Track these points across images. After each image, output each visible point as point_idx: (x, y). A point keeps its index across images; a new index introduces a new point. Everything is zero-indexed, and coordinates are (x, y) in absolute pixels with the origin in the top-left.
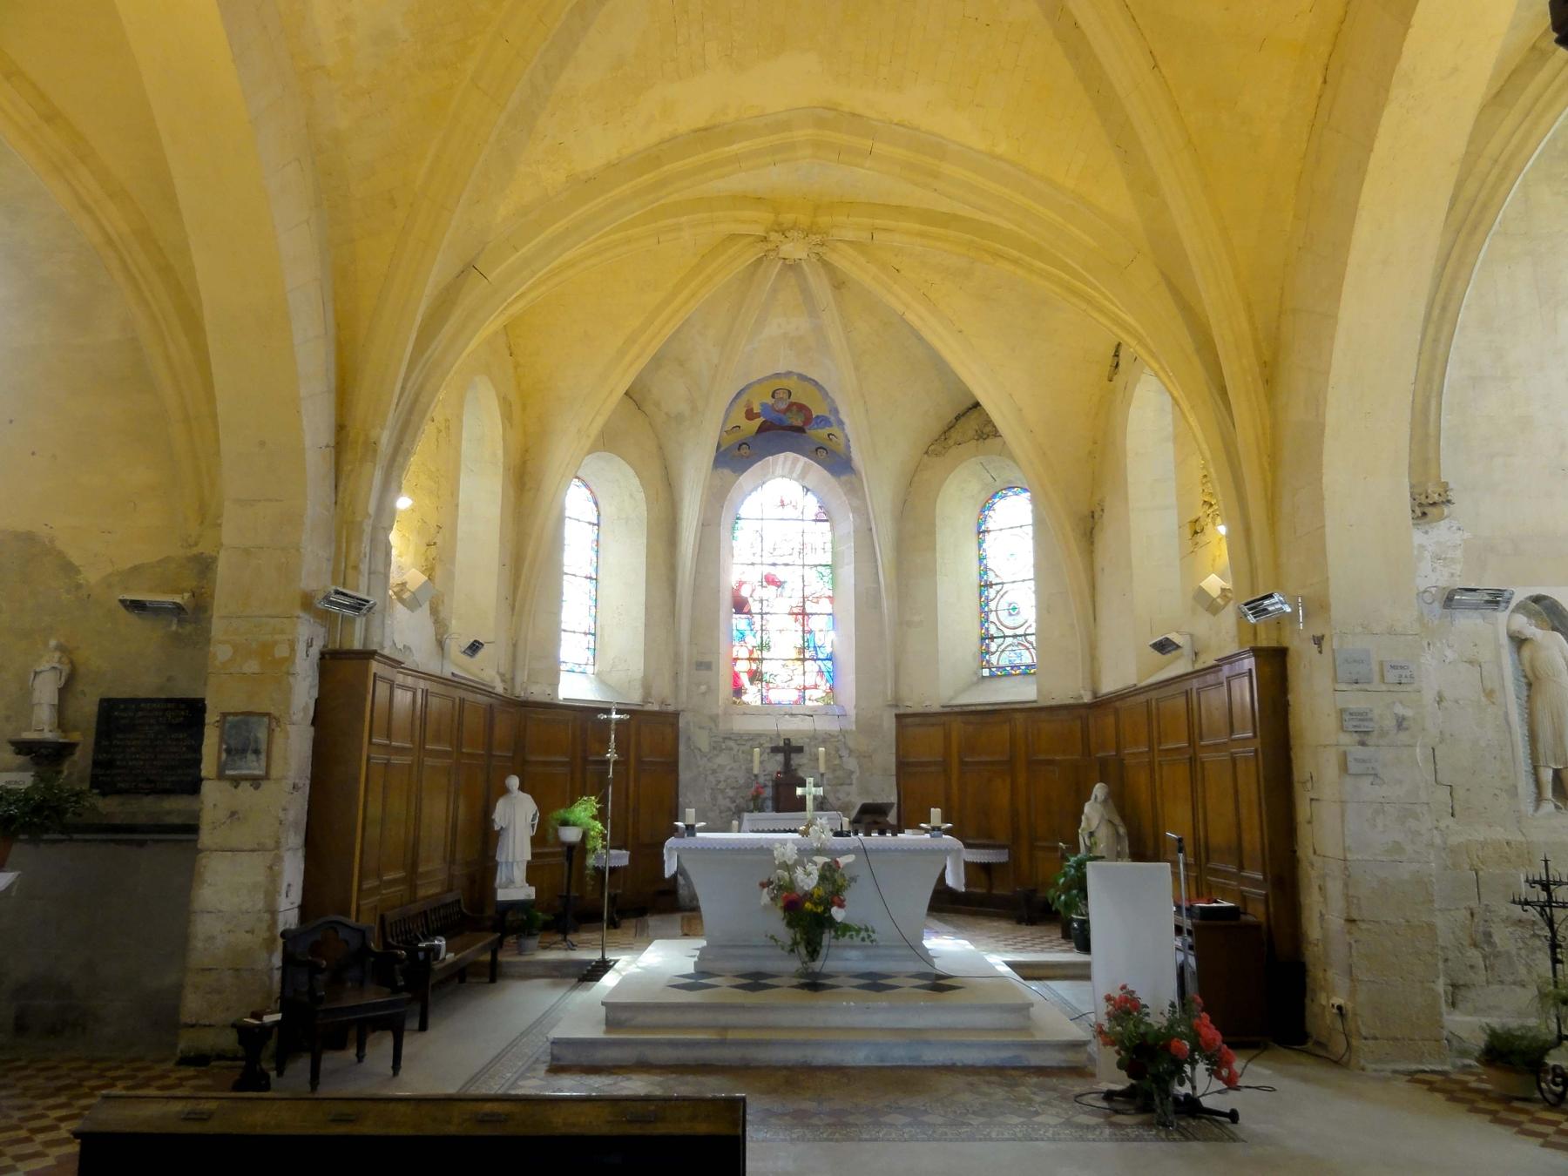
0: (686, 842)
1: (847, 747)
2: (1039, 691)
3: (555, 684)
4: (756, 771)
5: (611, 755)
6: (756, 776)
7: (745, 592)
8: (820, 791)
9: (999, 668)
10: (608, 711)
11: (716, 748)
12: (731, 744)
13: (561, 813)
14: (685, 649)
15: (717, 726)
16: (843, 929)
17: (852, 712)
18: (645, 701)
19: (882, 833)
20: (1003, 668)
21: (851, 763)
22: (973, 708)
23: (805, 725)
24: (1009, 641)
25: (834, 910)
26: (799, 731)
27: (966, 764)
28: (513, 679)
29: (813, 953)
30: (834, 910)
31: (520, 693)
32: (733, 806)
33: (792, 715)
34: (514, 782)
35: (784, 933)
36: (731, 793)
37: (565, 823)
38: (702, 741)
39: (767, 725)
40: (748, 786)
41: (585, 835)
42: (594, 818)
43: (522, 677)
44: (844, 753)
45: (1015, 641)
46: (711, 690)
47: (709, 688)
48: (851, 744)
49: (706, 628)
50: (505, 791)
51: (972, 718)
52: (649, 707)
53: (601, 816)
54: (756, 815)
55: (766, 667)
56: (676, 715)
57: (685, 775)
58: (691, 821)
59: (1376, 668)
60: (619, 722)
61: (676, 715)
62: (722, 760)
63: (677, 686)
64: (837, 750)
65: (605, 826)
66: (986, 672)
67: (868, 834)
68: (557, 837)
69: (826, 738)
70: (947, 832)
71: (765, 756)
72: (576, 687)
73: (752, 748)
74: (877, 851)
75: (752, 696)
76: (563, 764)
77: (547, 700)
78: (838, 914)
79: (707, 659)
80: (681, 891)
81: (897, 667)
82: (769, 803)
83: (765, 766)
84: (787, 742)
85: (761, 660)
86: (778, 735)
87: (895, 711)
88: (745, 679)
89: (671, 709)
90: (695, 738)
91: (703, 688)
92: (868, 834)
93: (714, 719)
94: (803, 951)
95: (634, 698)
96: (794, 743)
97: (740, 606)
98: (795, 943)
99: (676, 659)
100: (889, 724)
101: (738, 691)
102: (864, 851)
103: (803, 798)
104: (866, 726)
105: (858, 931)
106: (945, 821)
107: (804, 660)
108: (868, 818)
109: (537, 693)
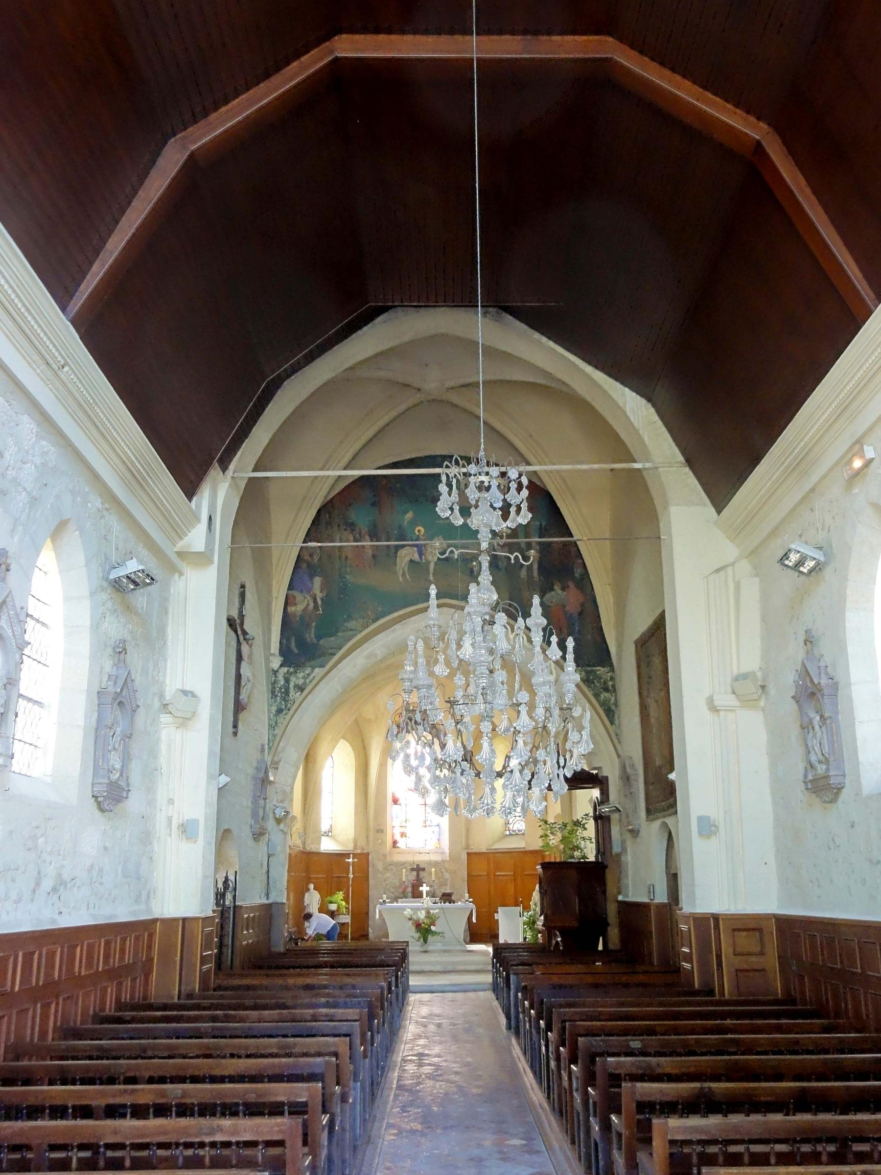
0: (383, 907)
1: (445, 868)
2: (526, 843)
3: (319, 843)
4: (404, 880)
5: (351, 876)
6: (404, 882)
7: (397, 796)
8: (428, 889)
9: (513, 831)
10: (347, 855)
11: (386, 869)
12: (392, 867)
13: (329, 898)
14: (372, 824)
15: (386, 858)
16: (434, 933)
17: (447, 851)
18: (355, 847)
19: (450, 903)
20: (515, 831)
21: (447, 876)
22: (499, 851)
23: (426, 858)
24: (517, 818)
25: (432, 927)
26: (423, 861)
27: (495, 875)
28: (305, 843)
29: (425, 941)
30: (432, 927)
31: (308, 849)
32: (393, 896)
33: (420, 853)
34: (312, 886)
35: (417, 935)
36: (393, 890)
37: (331, 902)
38: (380, 866)
39: (409, 858)
40: (401, 886)
41: (338, 907)
42: (342, 900)
43: (308, 842)
44: (443, 870)
45: (520, 819)
46: (383, 843)
47: (382, 841)
48: (446, 866)
49: (381, 811)
50: (308, 890)
51: (498, 855)
52: (356, 852)
53: (346, 899)
54: (404, 899)
55: (406, 831)
56: (368, 854)
57: (371, 882)
58: (385, 899)
59: (590, 850)
60: (353, 862)
61: (368, 854)
62: (388, 875)
63: (368, 840)
64: (440, 869)
65: (347, 903)
66: (508, 833)
67: (444, 903)
68: (327, 906)
69: (435, 864)
70: (470, 902)
71: (408, 873)
72: (327, 846)
73: (402, 869)
74: (447, 908)
75: (401, 844)
76: (323, 878)
77: (316, 850)
78: (433, 928)
79: (382, 828)
80: (370, 935)
81: (468, 830)
82: (410, 895)
83: (408, 877)
84: (418, 866)
85: (406, 827)
86: (414, 863)
87: (467, 851)
88: (397, 837)
89: (365, 851)
90: (376, 864)
91: (380, 841)
92: (444, 903)
93: (385, 856)
94: (422, 940)
95: (350, 847)
96: (421, 866)
97: (395, 801)
98: (420, 938)
99: (368, 829)
100: (464, 857)
101: (395, 843)
102: (442, 909)
103: (421, 892)
104: (453, 857)
105: (439, 933)
106: (470, 898)
107: (425, 826)
108: (445, 898)
109: (311, 847)
